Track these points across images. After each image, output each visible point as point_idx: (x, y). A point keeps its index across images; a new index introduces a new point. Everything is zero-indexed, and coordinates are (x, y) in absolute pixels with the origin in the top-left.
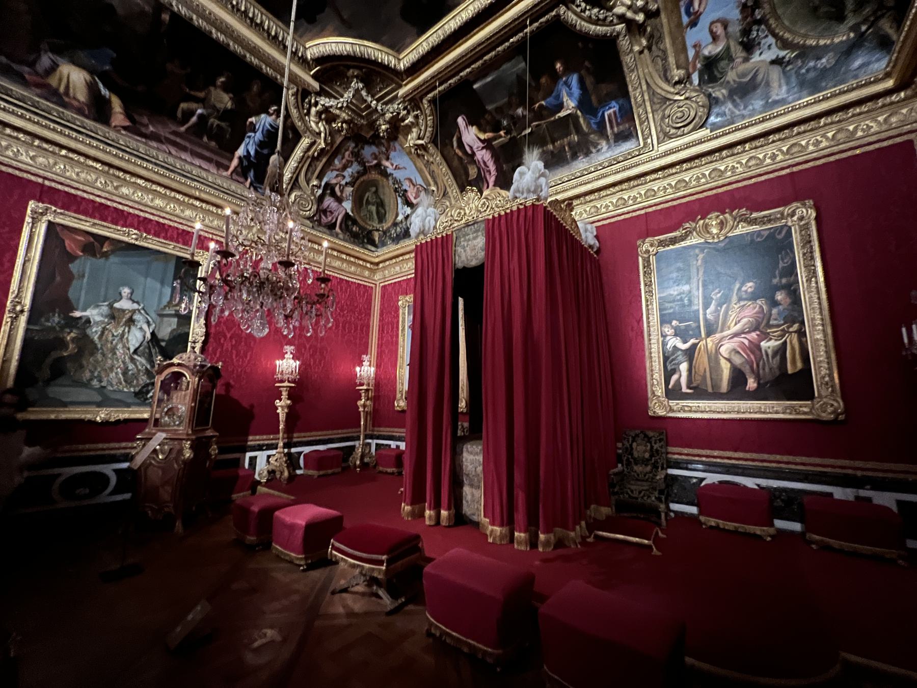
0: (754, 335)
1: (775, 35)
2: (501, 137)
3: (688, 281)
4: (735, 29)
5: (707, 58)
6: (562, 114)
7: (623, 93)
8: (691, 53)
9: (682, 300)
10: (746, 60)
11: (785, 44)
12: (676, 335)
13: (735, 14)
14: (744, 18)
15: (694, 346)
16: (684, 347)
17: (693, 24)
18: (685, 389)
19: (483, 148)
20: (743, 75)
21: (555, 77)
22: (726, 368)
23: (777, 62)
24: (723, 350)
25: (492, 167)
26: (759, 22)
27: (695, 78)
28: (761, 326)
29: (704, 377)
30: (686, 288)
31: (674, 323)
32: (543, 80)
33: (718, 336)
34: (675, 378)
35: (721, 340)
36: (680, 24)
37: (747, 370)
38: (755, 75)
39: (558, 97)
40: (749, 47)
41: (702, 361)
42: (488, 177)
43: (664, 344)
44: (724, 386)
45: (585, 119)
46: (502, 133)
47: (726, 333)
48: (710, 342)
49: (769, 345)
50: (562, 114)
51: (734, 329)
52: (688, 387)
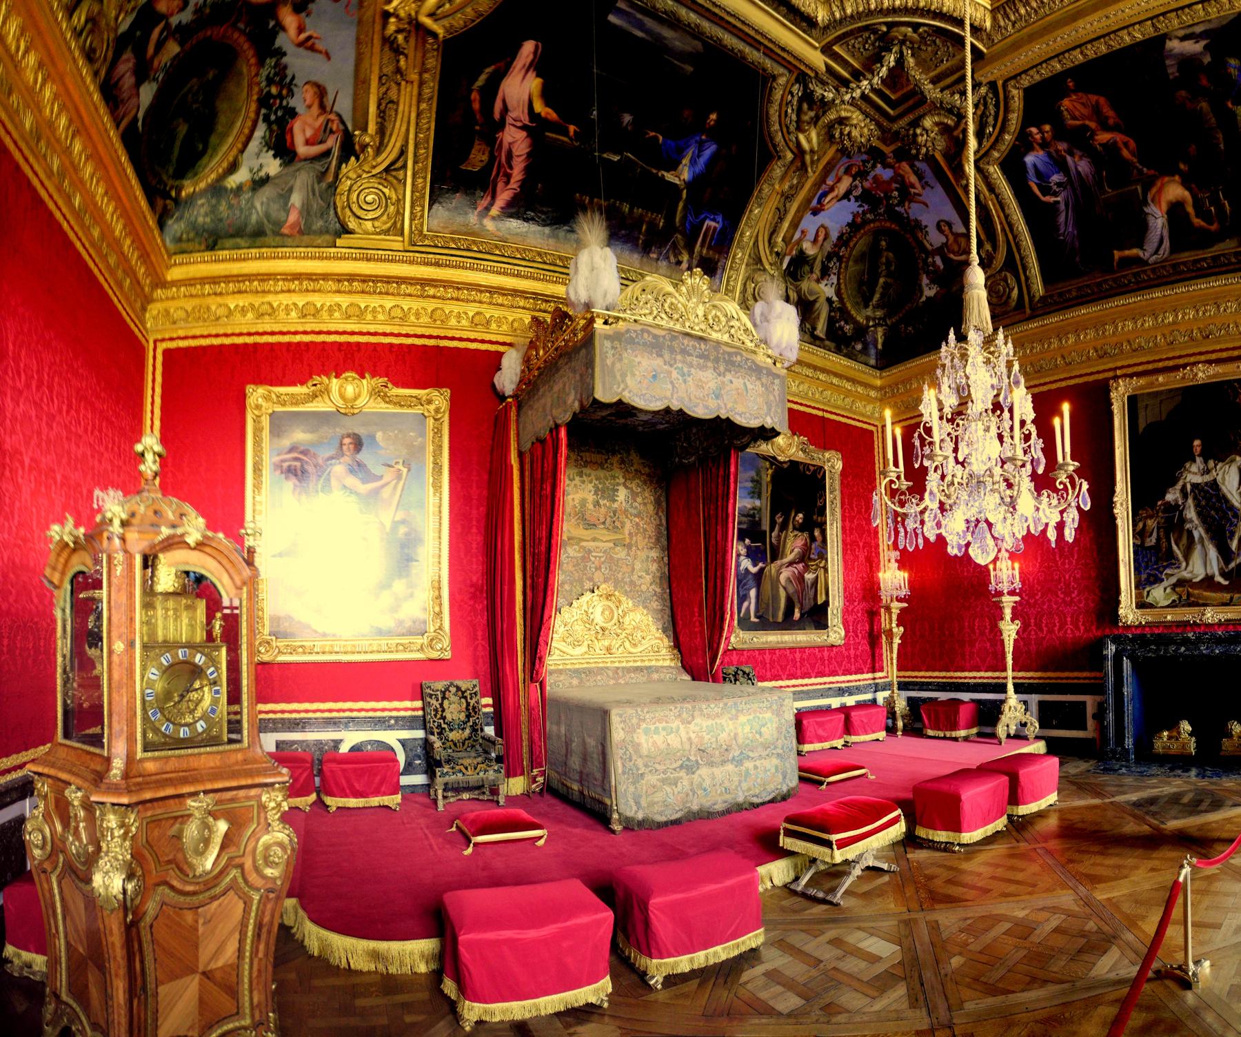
0: (801, 566)
1: (839, 279)
3: (759, 497)
9: (753, 516)
10: (818, 281)
12: (748, 556)
14: (835, 245)
15: (762, 570)
16: (754, 570)
18: (753, 619)
20: (811, 292)
22: (783, 594)
23: (829, 300)
24: (783, 578)
26: (840, 259)
28: (804, 558)
29: (768, 605)
30: (758, 503)
31: (747, 541)
33: (779, 562)
34: (745, 604)
35: (781, 567)
37: (796, 601)
38: (815, 301)
40: (825, 273)
41: (767, 586)
43: (738, 565)
44: (780, 618)
47: (786, 560)
48: (773, 567)
49: (809, 577)
51: (790, 557)
52: (756, 617)
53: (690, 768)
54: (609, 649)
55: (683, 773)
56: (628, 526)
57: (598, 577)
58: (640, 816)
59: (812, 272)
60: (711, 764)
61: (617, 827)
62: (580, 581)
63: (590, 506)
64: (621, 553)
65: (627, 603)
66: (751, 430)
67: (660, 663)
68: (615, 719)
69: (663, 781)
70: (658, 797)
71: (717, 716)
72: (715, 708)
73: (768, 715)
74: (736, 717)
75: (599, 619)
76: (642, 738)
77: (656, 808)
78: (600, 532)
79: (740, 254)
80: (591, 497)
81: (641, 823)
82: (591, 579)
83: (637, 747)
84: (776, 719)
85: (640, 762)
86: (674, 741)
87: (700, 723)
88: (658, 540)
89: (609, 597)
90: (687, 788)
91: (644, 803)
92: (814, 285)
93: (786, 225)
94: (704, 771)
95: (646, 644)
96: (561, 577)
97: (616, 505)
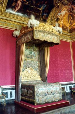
2: (27, 3)
4: (62, 17)
5: (58, 18)
6: (40, 9)
7: (48, 14)
8: (57, 16)
11: (63, 23)
13: (63, 15)
17: (60, 13)
19: (21, 2)
21: (44, 3)
23: (62, 24)
25: (19, 7)
27: (56, 19)
32: (43, 2)
36: (59, 11)
39: (41, 6)
40: (61, 20)
42: (17, 8)
45: (42, 13)
46: (28, 2)
50: (40, 9)
53: (46, 95)
54: (30, 77)
55: (45, 96)
56: (34, 58)
57: (29, 66)
58: (39, 102)
59: (59, 20)
60: (49, 95)
61: (36, 104)
62: (26, 66)
63: (28, 55)
64: (33, 62)
65: (34, 70)
66: (55, 43)
67: (38, 80)
68: (35, 88)
69: (42, 97)
70: (41, 100)
71: (50, 87)
72: (50, 85)
73: (58, 87)
74: (53, 87)
75: (29, 73)
76: (39, 90)
77: (41, 101)
78: (29, 59)
79: (49, 19)
80: (28, 53)
81: (39, 104)
82: (28, 66)
83: (38, 92)
84: (59, 88)
85: (39, 94)
86: (44, 91)
87: (47, 88)
88: (38, 60)
89: (31, 69)
90: (46, 98)
91: (39, 100)
92: (60, 22)
93: (56, 14)
94: (48, 96)
95: (36, 77)
96: (22, 66)
97: (32, 55)
